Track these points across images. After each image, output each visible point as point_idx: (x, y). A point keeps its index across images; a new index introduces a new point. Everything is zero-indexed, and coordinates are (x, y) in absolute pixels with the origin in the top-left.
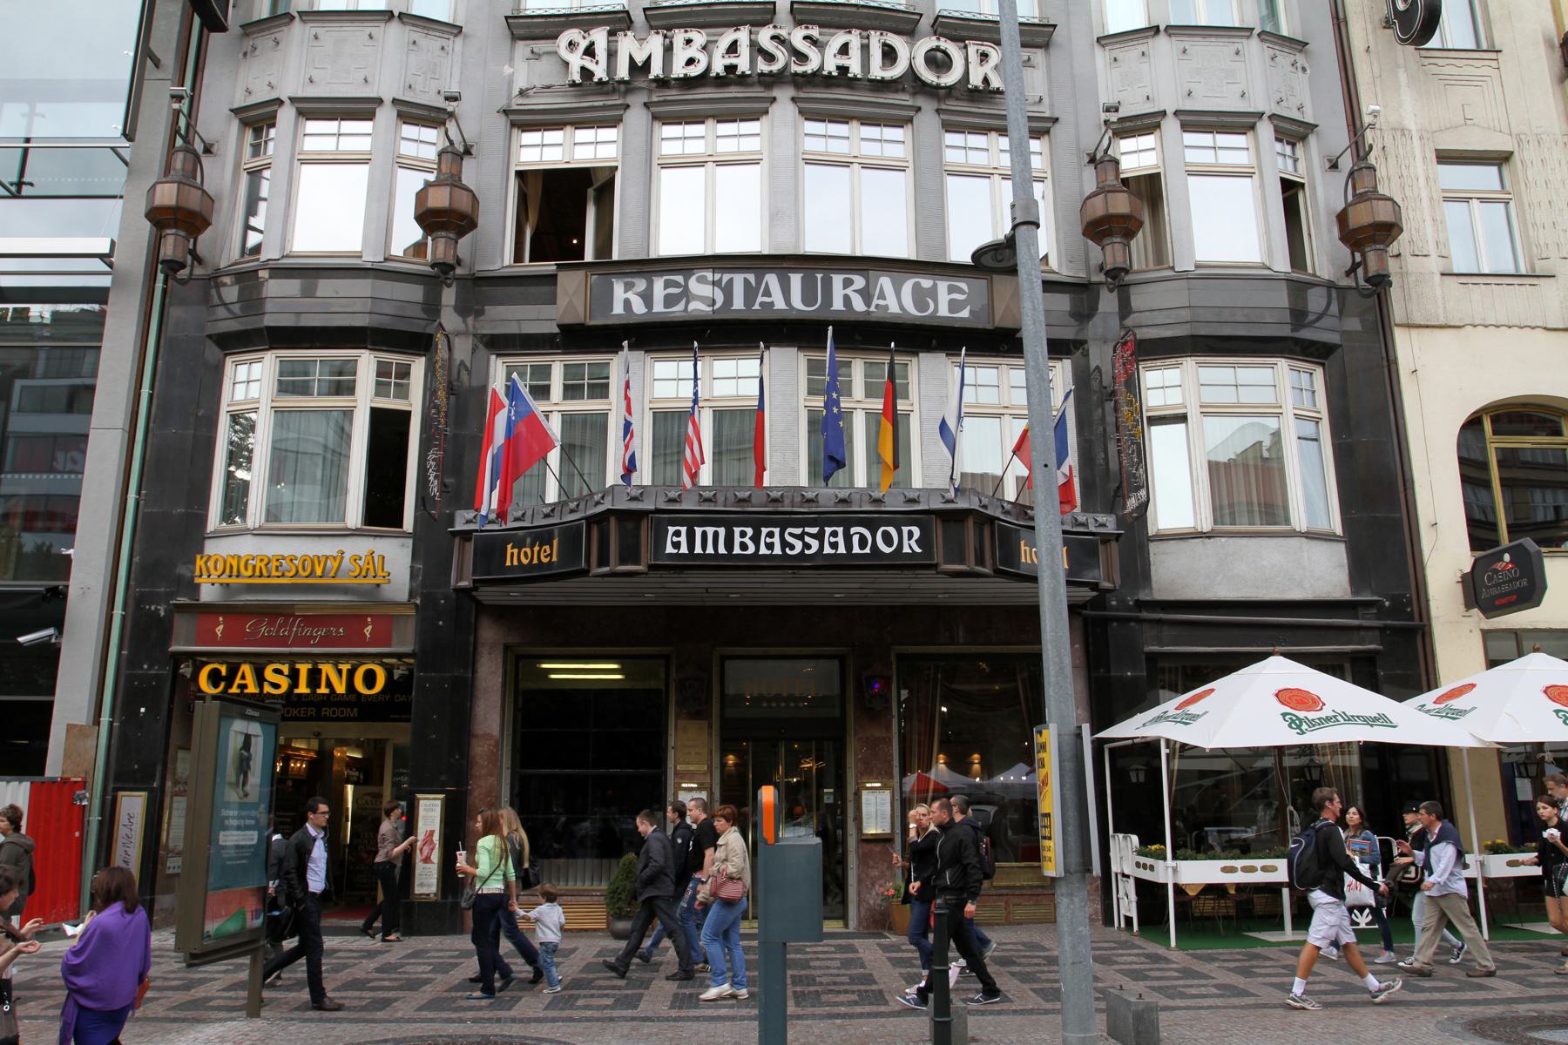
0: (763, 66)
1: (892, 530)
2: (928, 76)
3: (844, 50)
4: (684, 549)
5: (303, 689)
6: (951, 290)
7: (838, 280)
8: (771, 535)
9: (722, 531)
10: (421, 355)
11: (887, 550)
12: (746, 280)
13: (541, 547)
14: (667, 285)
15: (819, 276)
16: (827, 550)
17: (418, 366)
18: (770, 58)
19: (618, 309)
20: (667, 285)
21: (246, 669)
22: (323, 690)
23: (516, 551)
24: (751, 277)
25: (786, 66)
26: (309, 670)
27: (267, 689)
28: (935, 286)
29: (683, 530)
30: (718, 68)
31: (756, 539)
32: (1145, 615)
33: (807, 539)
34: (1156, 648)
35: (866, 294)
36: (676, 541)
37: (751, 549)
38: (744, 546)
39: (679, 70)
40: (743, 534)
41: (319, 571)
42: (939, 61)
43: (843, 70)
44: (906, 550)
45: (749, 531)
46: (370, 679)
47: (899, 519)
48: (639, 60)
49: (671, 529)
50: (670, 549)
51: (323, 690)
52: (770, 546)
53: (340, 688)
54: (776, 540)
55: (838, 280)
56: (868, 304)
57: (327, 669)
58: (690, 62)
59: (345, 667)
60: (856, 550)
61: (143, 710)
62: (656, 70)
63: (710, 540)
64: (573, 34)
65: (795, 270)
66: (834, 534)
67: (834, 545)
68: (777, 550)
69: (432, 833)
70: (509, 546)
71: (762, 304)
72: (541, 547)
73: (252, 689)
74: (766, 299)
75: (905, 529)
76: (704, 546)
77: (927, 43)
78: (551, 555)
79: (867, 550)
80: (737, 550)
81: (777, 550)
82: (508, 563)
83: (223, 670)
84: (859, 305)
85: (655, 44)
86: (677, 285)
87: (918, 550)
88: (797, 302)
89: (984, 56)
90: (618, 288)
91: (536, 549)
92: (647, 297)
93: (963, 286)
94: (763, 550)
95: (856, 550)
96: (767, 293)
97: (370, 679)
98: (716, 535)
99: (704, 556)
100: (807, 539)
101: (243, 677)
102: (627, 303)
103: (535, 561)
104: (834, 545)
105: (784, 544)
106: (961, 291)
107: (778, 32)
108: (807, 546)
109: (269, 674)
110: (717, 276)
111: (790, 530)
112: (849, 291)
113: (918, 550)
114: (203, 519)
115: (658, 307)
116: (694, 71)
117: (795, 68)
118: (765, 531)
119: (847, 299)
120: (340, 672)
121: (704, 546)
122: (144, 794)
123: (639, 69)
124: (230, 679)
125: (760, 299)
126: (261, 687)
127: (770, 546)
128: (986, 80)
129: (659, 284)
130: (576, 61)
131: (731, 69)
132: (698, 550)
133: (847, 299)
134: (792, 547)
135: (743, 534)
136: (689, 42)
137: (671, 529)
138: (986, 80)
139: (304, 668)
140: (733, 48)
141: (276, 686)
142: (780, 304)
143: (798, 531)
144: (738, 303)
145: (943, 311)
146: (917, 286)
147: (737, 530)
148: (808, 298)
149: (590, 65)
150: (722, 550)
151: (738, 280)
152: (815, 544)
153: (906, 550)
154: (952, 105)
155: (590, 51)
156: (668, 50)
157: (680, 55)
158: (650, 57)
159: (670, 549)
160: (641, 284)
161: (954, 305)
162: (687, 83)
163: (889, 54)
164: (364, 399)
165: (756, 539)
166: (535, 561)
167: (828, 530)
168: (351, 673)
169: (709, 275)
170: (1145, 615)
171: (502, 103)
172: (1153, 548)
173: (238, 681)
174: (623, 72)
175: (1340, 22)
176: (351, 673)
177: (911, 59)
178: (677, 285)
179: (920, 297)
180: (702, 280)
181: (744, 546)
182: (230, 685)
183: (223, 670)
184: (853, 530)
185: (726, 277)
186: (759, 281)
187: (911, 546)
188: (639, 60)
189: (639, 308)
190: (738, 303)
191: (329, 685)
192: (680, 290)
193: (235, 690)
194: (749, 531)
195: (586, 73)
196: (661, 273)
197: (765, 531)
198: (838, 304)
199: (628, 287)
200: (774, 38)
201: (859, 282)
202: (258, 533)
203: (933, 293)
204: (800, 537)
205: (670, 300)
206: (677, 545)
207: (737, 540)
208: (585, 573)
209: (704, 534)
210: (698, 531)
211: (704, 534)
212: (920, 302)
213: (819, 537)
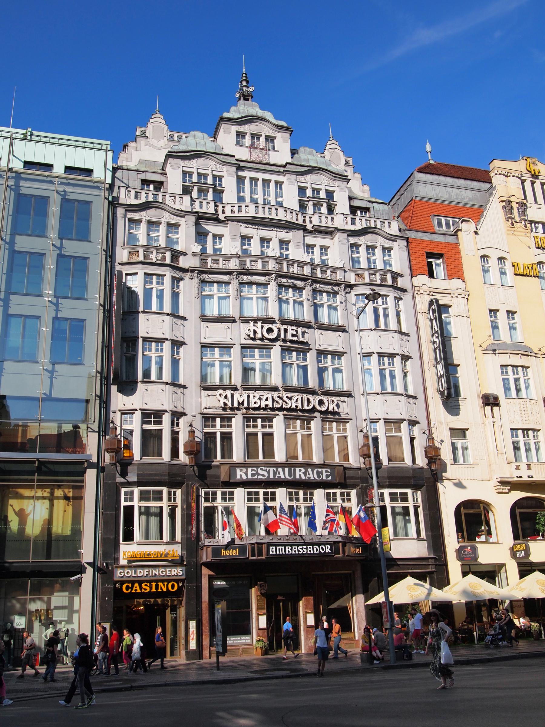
0: (276, 405)
1: (323, 546)
4: (274, 553)
5: (154, 590)
6: (326, 472)
7: (297, 469)
8: (295, 548)
9: (283, 548)
10: (179, 489)
11: (323, 552)
12: (273, 470)
13: (233, 550)
14: (252, 470)
15: (293, 469)
16: (309, 552)
17: (179, 492)
19: (238, 477)
20: (252, 470)
21: (137, 585)
22: (160, 590)
23: (225, 551)
24: (275, 469)
25: (282, 406)
26: (155, 585)
27: (143, 590)
28: (322, 470)
29: (274, 547)
30: (263, 406)
31: (291, 549)
33: (304, 549)
35: (305, 473)
36: (273, 550)
37: (290, 552)
38: (289, 552)
39: (252, 405)
40: (288, 548)
41: (159, 556)
42: (321, 403)
43: (297, 406)
44: (327, 552)
45: (290, 547)
46: (173, 586)
47: (325, 544)
48: (241, 401)
49: (271, 547)
50: (271, 553)
51: (160, 590)
52: (295, 551)
53: (165, 590)
54: (296, 550)
55: (297, 469)
56: (306, 477)
57: (160, 584)
58: (255, 403)
59: (166, 583)
60: (315, 552)
61: (107, 598)
62: (246, 405)
63: (281, 550)
64: (220, 391)
65: (286, 467)
66: (310, 548)
67: (310, 551)
68: (297, 552)
69: (194, 631)
70: (222, 550)
71: (278, 477)
72: (233, 550)
73: (139, 591)
74: (279, 475)
75: (326, 546)
76: (279, 552)
78: (236, 553)
79: (318, 552)
80: (287, 553)
81: (297, 552)
82: (222, 555)
83: (130, 585)
84: (303, 477)
85: (245, 397)
86: (255, 470)
87: (330, 552)
88: (287, 477)
90: (238, 471)
91: (231, 551)
92: (246, 474)
93: (329, 470)
94: (293, 553)
95: (315, 552)
96: (279, 474)
97: (173, 586)
98: (282, 548)
99: (279, 554)
100: (304, 549)
101: (136, 587)
102: (241, 476)
103: (231, 554)
104: (310, 551)
105: (298, 551)
106: (329, 472)
107: (279, 395)
108: (304, 551)
109: (143, 585)
110: (266, 468)
111: (299, 547)
112: (300, 473)
113: (330, 552)
114: (119, 540)
115: (250, 477)
116: (257, 406)
117: (286, 407)
118: (293, 547)
119: (300, 475)
120: (164, 585)
121: (279, 552)
122: (109, 623)
123: (241, 404)
124: (132, 588)
125: (277, 475)
126: (141, 589)
127: (295, 551)
128: (333, 409)
129: (249, 470)
130: (223, 400)
132: (278, 553)
133: (300, 475)
134: (300, 552)
135: (288, 548)
136: (254, 396)
137: (271, 547)
138: (333, 409)
139: (154, 584)
140: (267, 399)
141: (146, 589)
142: (283, 477)
143: (301, 547)
144: (272, 476)
145: (324, 478)
146: (318, 471)
147: (287, 547)
148: (290, 475)
149: (226, 402)
150: (284, 553)
151: (271, 469)
152: (305, 550)
153: (327, 552)
155: (226, 397)
156: (248, 397)
157: (252, 401)
158: (243, 401)
159: (271, 553)
160: (244, 470)
161: (327, 476)
162: (254, 409)
163: (308, 401)
164: (165, 504)
165: (291, 549)
166: (231, 554)
167: (308, 547)
168: (167, 585)
169: (264, 468)
171: (199, 411)
173: (134, 588)
174: (236, 405)
175: (425, 389)
176: (167, 585)
178: (255, 470)
179: (319, 474)
180: (262, 469)
181: (289, 552)
182: (132, 590)
183: (130, 585)
184: (314, 547)
185: (268, 469)
186: (277, 470)
187: (328, 551)
188: (241, 401)
189: (244, 477)
190: (272, 476)
191: (161, 589)
192: (255, 472)
193: (133, 591)
194: (290, 547)
195: (225, 404)
196: (250, 467)
197: (293, 547)
198: (298, 477)
199: (241, 471)
200: (279, 397)
201: (303, 470)
202: (139, 543)
203: (321, 473)
204: (302, 549)
205: (253, 475)
206: (273, 552)
207: (287, 550)
208: (248, 558)
209: (279, 548)
210: (278, 548)
211: (279, 548)
212: (319, 477)
213: (306, 548)
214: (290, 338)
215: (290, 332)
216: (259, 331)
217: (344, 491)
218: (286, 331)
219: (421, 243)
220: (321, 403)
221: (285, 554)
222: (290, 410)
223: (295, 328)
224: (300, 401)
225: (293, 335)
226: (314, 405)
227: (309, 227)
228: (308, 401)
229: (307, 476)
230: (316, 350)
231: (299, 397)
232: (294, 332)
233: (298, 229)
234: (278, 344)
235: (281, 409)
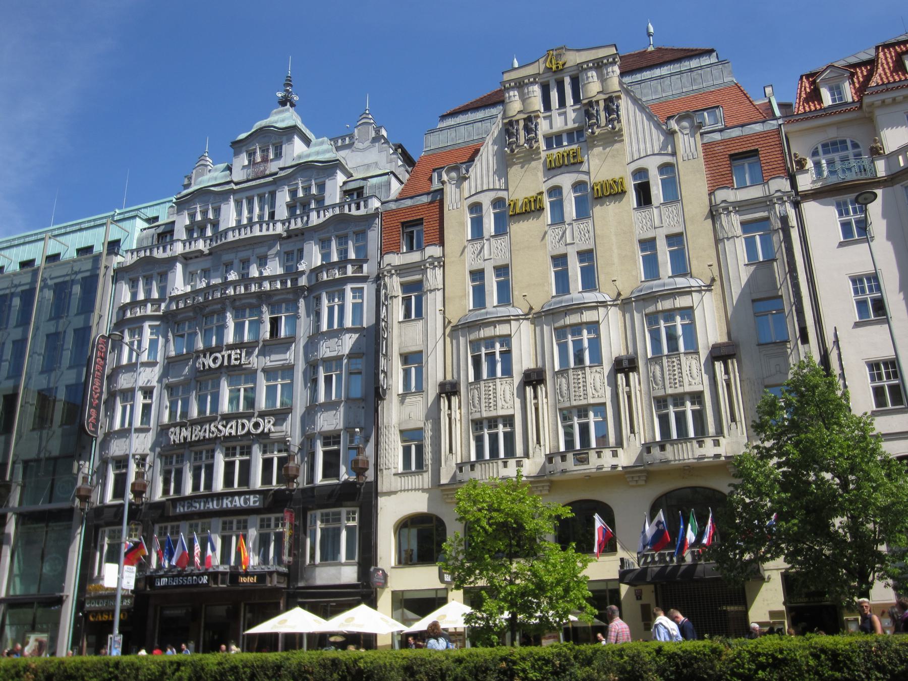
2: (253, 431)
3: (231, 427)
35: (231, 502)
42: (256, 425)
43: (230, 434)
56: (231, 504)
62: (189, 439)
84: (229, 505)
89: (269, 422)
119: (227, 504)
123: (185, 439)
138: (269, 430)
142: (211, 507)
145: (252, 504)
148: (218, 505)
161: (255, 502)
163: (243, 425)
174: (182, 441)
179: (245, 501)
190: (202, 508)
198: (225, 506)
203: (249, 499)
212: (245, 502)
214: (233, 362)
215: (233, 357)
218: (230, 356)
223: (238, 351)
224: (234, 427)
225: (236, 359)
229: (234, 504)
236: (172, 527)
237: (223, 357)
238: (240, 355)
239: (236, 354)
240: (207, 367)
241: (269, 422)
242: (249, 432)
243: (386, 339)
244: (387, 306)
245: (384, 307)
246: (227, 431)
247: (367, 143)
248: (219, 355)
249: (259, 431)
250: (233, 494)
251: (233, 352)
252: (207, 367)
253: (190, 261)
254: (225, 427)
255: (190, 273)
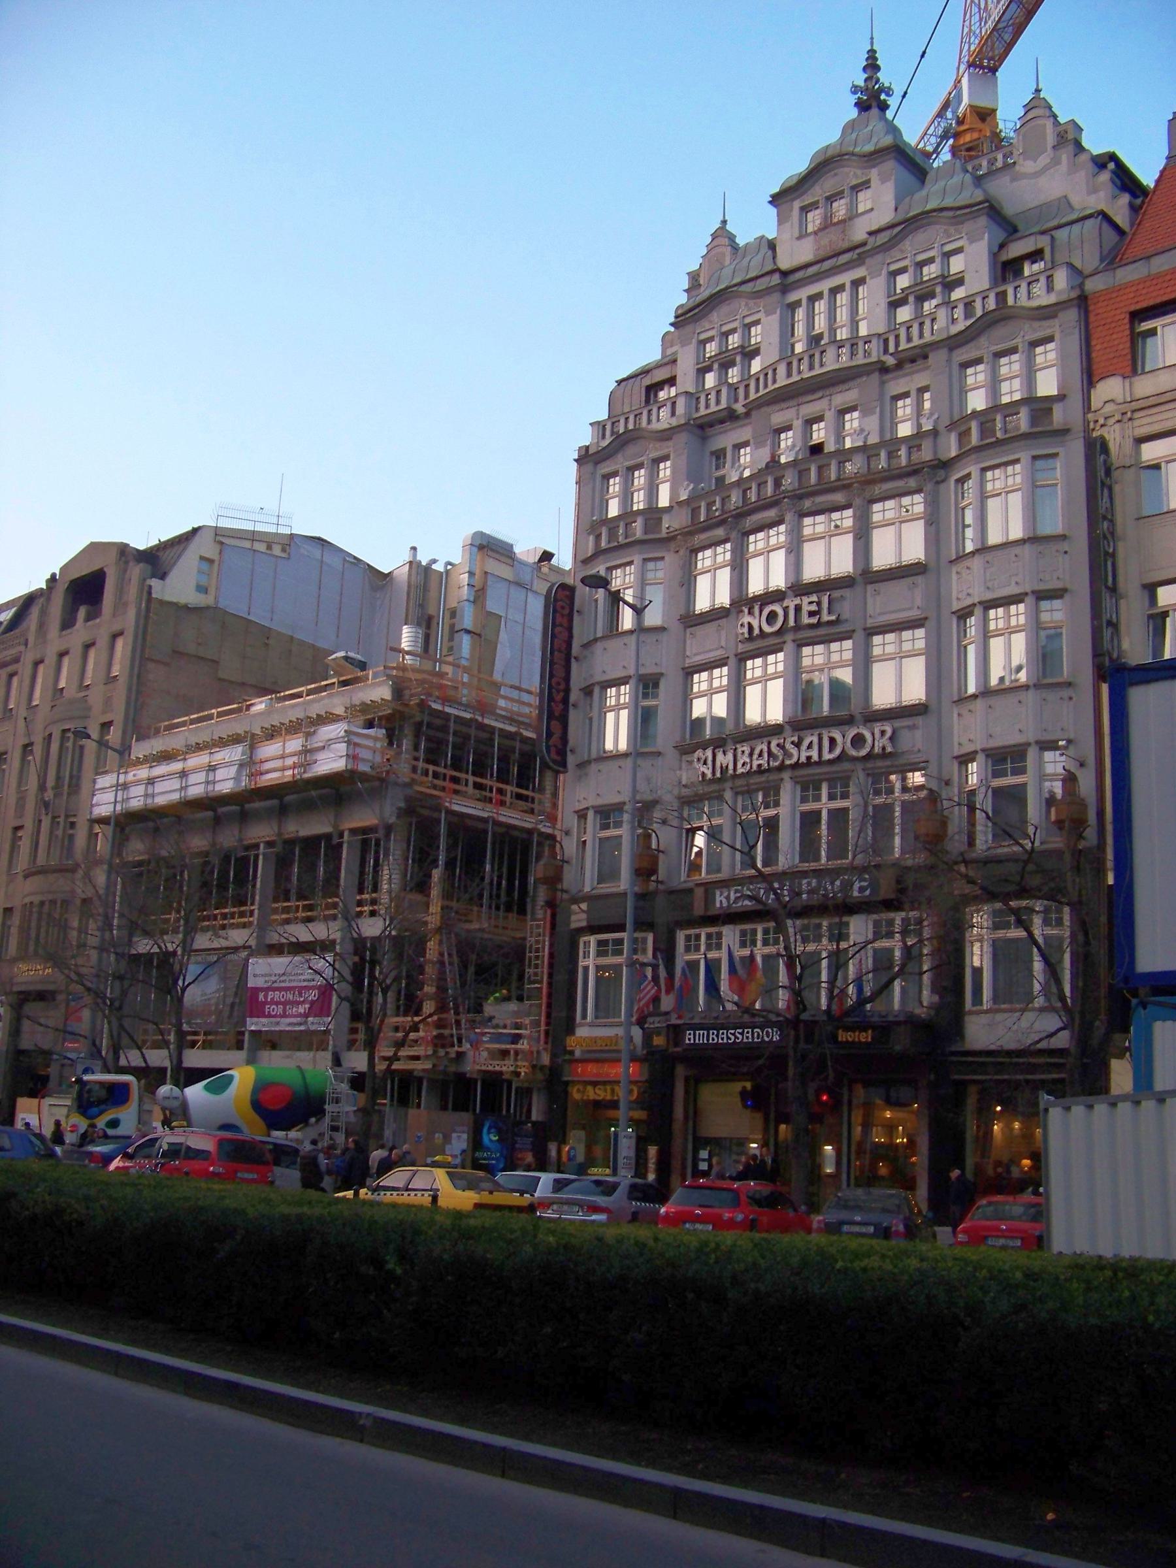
2: (854, 753)
3: (810, 746)
11: (766, 1039)
14: (736, 891)
17: (650, 938)
18: (775, 757)
19: (718, 905)
20: (736, 891)
25: (783, 761)
31: (717, 1036)
32: (954, 1059)
34: (956, 1077)
39: (740, 770)
42: (858, 740)
43: (809, 758)
62: (731, 772)
77: (852, 732)
90: (718, 893)
105: (728, 1038)
106: (865, 880)
117: (788, 762)
123: (724, 770)
128: (884, 748)
131: (760, 766)
138: (884, 748)
140: (760, 755)
145: (856, 894)
154: (869, 765)
161: (861, 889)
163: (832, 741)
165: (717, 1036)
170: (954, 1059)
172: (967, 1019)
174: (718, 775)
177: (844, 743)
187: (776, 1038)
200: (778, 745)
204: (733, 1034)
213: (742, 1034)
214: (806, 620)
215: (806, 608)
216: (755, 624)
217: (688, 932)
218: (798, 609)
219: (1121, 293)
220: (858, 740)
221: (708, 1044)
222: (796, 766)
223: (814, 598)
224: (816, 747)
225: (811, 614)
226: (843, 750)
227: (890, 361)
228: (832, 741)
230: (865, 629)
231: (815, 739)
232: (814, 608)
233: (868, 374)
234: (789, 637)
235: (782, 768)
236: (709, 936)
237: (786, 610)
238: (819, 604)
239: (811, 603)
240: (756, 631)
241: (883, 733)
242: (843, 757)
243: (1113, 555)
244: (1110, 489)
245: (1106, 492)
246: (798, 755)
247: (1044, 160)
248: (777, 608)
249: (863, 752)
250: (818, 873)
251: (806, 600)
252: (756, 631)
253: (710, 431)
254: (798, 745)
255: (712, 453)
